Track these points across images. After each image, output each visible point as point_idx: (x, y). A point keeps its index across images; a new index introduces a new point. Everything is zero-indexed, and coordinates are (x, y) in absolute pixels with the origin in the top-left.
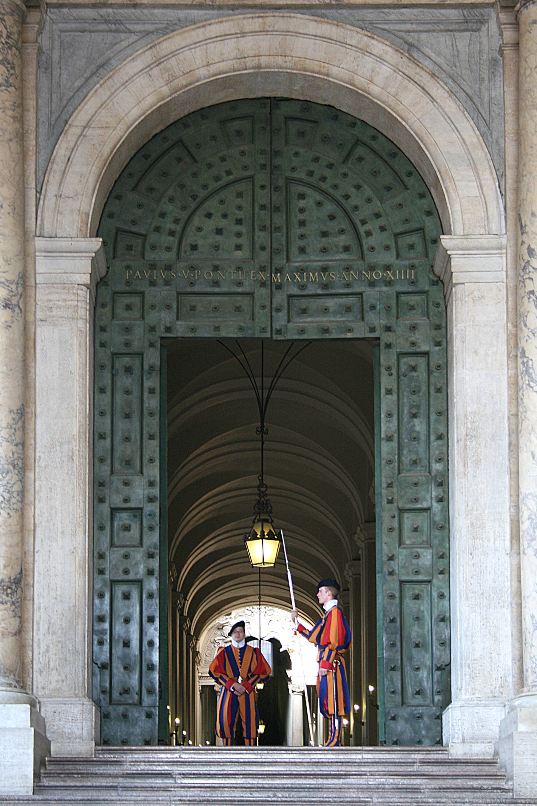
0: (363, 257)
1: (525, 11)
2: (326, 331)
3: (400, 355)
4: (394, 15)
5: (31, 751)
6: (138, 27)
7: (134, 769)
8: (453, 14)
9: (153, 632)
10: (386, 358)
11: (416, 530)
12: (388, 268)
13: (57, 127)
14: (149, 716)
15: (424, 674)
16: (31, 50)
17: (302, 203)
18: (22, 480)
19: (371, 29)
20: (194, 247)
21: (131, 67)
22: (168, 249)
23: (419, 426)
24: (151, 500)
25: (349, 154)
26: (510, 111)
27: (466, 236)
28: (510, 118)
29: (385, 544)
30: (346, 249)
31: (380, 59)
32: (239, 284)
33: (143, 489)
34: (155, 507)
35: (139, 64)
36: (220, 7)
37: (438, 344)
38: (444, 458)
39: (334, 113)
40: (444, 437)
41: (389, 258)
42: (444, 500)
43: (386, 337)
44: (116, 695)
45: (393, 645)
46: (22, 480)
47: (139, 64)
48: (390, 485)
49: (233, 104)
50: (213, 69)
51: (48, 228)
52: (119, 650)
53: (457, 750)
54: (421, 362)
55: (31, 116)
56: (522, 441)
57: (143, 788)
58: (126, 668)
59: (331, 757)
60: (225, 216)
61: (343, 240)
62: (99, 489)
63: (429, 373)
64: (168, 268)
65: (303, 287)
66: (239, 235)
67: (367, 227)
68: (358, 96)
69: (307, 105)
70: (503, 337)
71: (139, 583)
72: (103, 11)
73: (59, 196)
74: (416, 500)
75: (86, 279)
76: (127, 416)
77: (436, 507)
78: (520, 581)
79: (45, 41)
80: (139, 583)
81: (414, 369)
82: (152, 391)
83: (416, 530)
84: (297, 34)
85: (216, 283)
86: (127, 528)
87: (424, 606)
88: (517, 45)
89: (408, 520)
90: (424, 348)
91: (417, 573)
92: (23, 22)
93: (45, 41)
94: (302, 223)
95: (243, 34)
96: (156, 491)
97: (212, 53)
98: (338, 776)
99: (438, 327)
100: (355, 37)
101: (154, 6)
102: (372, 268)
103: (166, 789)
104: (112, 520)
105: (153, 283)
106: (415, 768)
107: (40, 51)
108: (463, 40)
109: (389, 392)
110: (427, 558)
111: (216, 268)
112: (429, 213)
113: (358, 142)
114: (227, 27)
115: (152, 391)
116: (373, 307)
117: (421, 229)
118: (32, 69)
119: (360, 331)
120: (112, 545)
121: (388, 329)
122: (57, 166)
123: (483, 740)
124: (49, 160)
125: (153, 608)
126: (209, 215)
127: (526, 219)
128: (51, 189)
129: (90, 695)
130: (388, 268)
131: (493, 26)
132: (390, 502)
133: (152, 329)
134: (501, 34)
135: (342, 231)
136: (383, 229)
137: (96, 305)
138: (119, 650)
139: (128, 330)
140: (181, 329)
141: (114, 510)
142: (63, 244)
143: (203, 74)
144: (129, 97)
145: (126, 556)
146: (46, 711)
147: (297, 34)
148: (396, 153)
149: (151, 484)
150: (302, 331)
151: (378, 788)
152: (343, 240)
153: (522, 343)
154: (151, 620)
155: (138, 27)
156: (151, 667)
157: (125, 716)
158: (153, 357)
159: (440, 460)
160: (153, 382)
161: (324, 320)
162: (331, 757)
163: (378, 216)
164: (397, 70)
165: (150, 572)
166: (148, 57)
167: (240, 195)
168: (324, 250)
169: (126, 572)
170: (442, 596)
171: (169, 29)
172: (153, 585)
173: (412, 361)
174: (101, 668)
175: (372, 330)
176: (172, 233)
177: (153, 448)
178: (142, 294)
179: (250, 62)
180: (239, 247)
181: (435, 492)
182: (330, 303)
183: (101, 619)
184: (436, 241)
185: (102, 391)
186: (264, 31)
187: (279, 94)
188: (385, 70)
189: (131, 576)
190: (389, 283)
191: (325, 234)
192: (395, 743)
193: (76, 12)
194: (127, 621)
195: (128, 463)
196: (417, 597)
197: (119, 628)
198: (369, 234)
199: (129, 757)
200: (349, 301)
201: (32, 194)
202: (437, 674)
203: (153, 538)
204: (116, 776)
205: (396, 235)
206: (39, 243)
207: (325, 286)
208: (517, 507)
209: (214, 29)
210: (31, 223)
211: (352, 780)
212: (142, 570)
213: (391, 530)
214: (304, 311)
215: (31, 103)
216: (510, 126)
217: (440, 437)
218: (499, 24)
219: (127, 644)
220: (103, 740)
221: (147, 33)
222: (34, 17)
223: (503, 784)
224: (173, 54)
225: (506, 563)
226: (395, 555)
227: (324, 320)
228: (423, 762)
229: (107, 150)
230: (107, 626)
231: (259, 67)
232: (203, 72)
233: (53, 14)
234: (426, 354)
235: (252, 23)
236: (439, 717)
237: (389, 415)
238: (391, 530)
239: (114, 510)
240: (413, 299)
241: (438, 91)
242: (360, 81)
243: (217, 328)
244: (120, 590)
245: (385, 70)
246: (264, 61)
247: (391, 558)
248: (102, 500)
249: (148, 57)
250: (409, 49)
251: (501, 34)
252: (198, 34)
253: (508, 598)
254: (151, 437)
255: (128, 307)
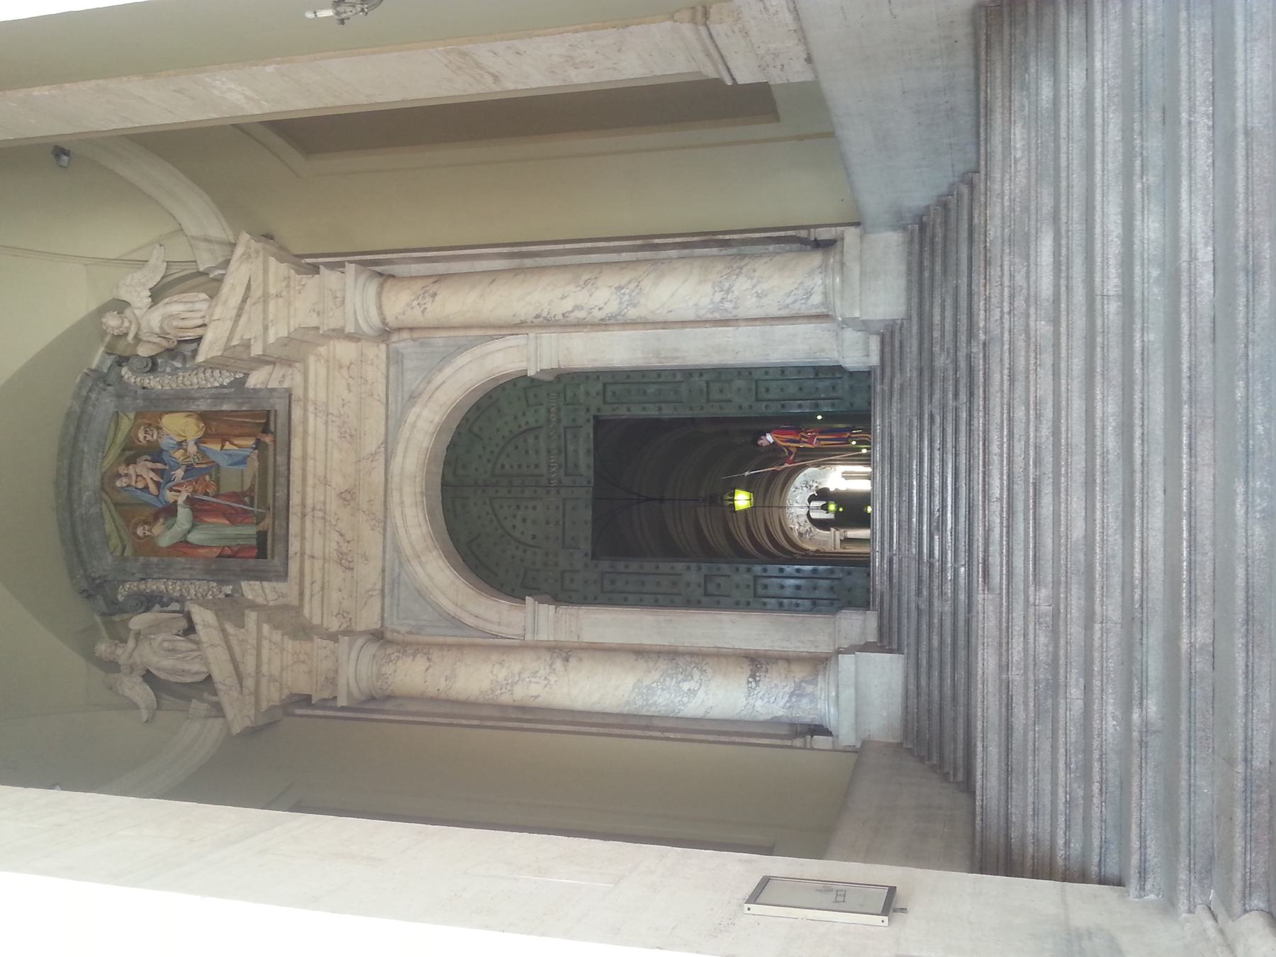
0: (541, 427)
1: (391, 324)
2: (588, 451)
3: (605, 402)
4: (392, 407)
5: (872, 655)
6: (397, 570)
7: (886, 583)
8: (392, 370)
9: (789, 569)
10: (607, 412)
11: (721, 391)
12: (549, 411)
13: (456, 623)
14: (849, 573)
15: (821, 385)
16: (410, 638)
17: (507, 467)
18: (683, 654)
19: (400, 422)
20: (534, 537)
21: (421, 573)
22: (535, 554)
23: (652, 389)
24: (699, 569)
25: (477, 436)
26: (452, 333)
27: (528, 360)
28: (456, 333)
29: (730, 411)
30: (536, 438)
31: (418, 416)
32: (558, 508)
33: (691, 574)
34: (704, 566)
35: (419, 569)
36: (385, 517)
37: (598, 378)
38: (673, 372)
39: (452, 446)
40: (659, 372)
41: (543, 410)
42: (701, 372)
43: (593, 411)
44: (834, 596)
45: (800, 406)
46: (683, 654)
47: (419, 569)
48: (691, 409)
49: (445, 510)
50: (423, 523)
51: (520, 632)
52: (803, 593)
53: (874, 360)
54: (609, 388)
55: (449, 640)
56: (660, 319)
57: (900, 577)
58: (815, 589)
59: (878, 447)
60: (514, 516)
61: (531, 441)
62: (690, 603)
63: (615, 383)
64: (547, 554)
65: (560, 466)
66: (527, 508)
67: (523, 424)
68: (441, 431)
69: (447, 463)
70: (593, 334)
71: (756, 578)
72: (387, 591)
73: (499, 624)
74: (701, 390)
75: (552, 607)
76: (643, 584)
77: (706, 377)
78: (756, 319)
79: (403, 629)
80: (756, 578)
81: (614, 393)
82: (627, 567)
83: (721, 391)
84: (403, 468)
85: (557, 523)
86: (719, 585)
87: (773, 385)
88: (411, 329)
89: (715, 395)
90: (600, 387)
91: (750, 390)
92: (391, 642)
93: (403, 629)
94: (520, 466)
95: (402, 502)
96: (693, 566)
97: (414, 522)
98: (891, 441)
99: (587, 378)
100: (405, 431)
101: (384, 559)
102: (549, 421)
103: (900, 561)
104: (712, 595)
105: (556, 564)
106: (886, 388)
107: (410, 633)
108: (409, 364)
109: (629, 410)
110: (740, 383)
111: (548, 523)
112: (515, 385)
113: (470, 431)
114: (397, 512)
115: (627, 567)
116: (574, 420)
117: (525, 389)
118: (421, 638)
119: (589, 429)
120: (728, 596)
121: (588, 410)
122: (481, 624)
123: (867, 344)
124: (476, 629)
125: (773, 569)
126: (514, 527)
127: (517, 321)
128: (495, 629)
129: (834, 613)
130: (549, 411)
131: (400, 345)
132: (702, 408)
133: (586, 565)
134: (405, 340)
135: (525, 441)
136: (524, 414)
137: (570, 601)
138: (803, 593)
139: (586, 582)
140: (586, 546)
141: (706, 594)
142: (530, 621)
143: (426, 528)
144: (438, 576)
145: (737, 586)
146: (845, 644)
147: (403, 468)
148: (477, 406)
149: (689, 568)
150: (589, 467)
151: (901, 411)
152: (531, 441)
153: (596, 321)
154: (781, 570)
155: (397, 570)
156: (814, 571)
157: (850, 590)
158: (605, 565)
159: (674, 376)
160: (620, 566)
161: (582, 452)
162: (878, 447)
163: (516, 418)
164: (426, 405)
165: (749, 570)
166: (415, 563)
167: (501, 507)
168: (537, 452)
169: (748, 586)
170: (767, 373)
171: (398, 550)
172: (758, 569)
173: (609, 394)
174: (815, 606)
175: (588, 421)
176: (525, 551)
177: (665, 567)
178: (563, 572)
179: (419, 499)
180: (534, 508)
181: (696, 378)
182: (571, 448)
183: (781, 604)
184: (532, 379)
185: (626, 599)
186: (401, 490)
187: (439, 480)
188: (425, 413)
189: (752, 583)
190: (559, 410)
191: (527, 452)
192: (870, 404)
193: (387, 609)
194: (782, 587)
195: (674, 584)
196: (767, 390)
197: (788, 592)
198: (527, 423)
199: (878, 587)
200: (569, 436)
201: (497, 641)
202: (821, 376)
203: (725, 568)
204: (891, 596)
205: (528, 405)
206: (529, 637)
207: (560, 451)
208: (706, 321)
209: (399, 521)
210: (516, 642)
211: (894, 431)
212: (747, 576)
213: (721, 408)
214: (576, 466)
215: (441, 640)
216: (461, 333)
217: (659, 376)
218: (399, 341)
219: (798, 587)
220: (865, 605)
221: (400, 564)
222: (388, 635)
223: (897, 327)
224: (413, 548)
225: (744, 330)
226: (737, 403)
227: (582, 452)
228: (882, 383)
229: (471, 592)
230: (785, 601)
231: (422, 493)
232: (424, 528)
233: (388, 624)
234: (604, 385)
235: (395, 498)
236: (852, 374)
237: (644, 409)
238: (721, 408)
239: (706, 594)
240: (569, 394)
241: (438, 379)
242: (431, 429)
243: (586, 523)
244: (760, 591)
245: (425, 413)
246: (418, 490)
247: (740, 407)
248: (699, 602)
249: (415, 563)
250: (413, 398)
251: (405, 340)
252: (402, 532)
253: (767, 328)
254: (657, 567)
255: (572, 581)
